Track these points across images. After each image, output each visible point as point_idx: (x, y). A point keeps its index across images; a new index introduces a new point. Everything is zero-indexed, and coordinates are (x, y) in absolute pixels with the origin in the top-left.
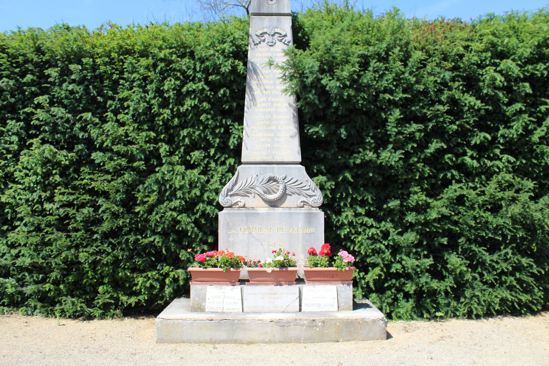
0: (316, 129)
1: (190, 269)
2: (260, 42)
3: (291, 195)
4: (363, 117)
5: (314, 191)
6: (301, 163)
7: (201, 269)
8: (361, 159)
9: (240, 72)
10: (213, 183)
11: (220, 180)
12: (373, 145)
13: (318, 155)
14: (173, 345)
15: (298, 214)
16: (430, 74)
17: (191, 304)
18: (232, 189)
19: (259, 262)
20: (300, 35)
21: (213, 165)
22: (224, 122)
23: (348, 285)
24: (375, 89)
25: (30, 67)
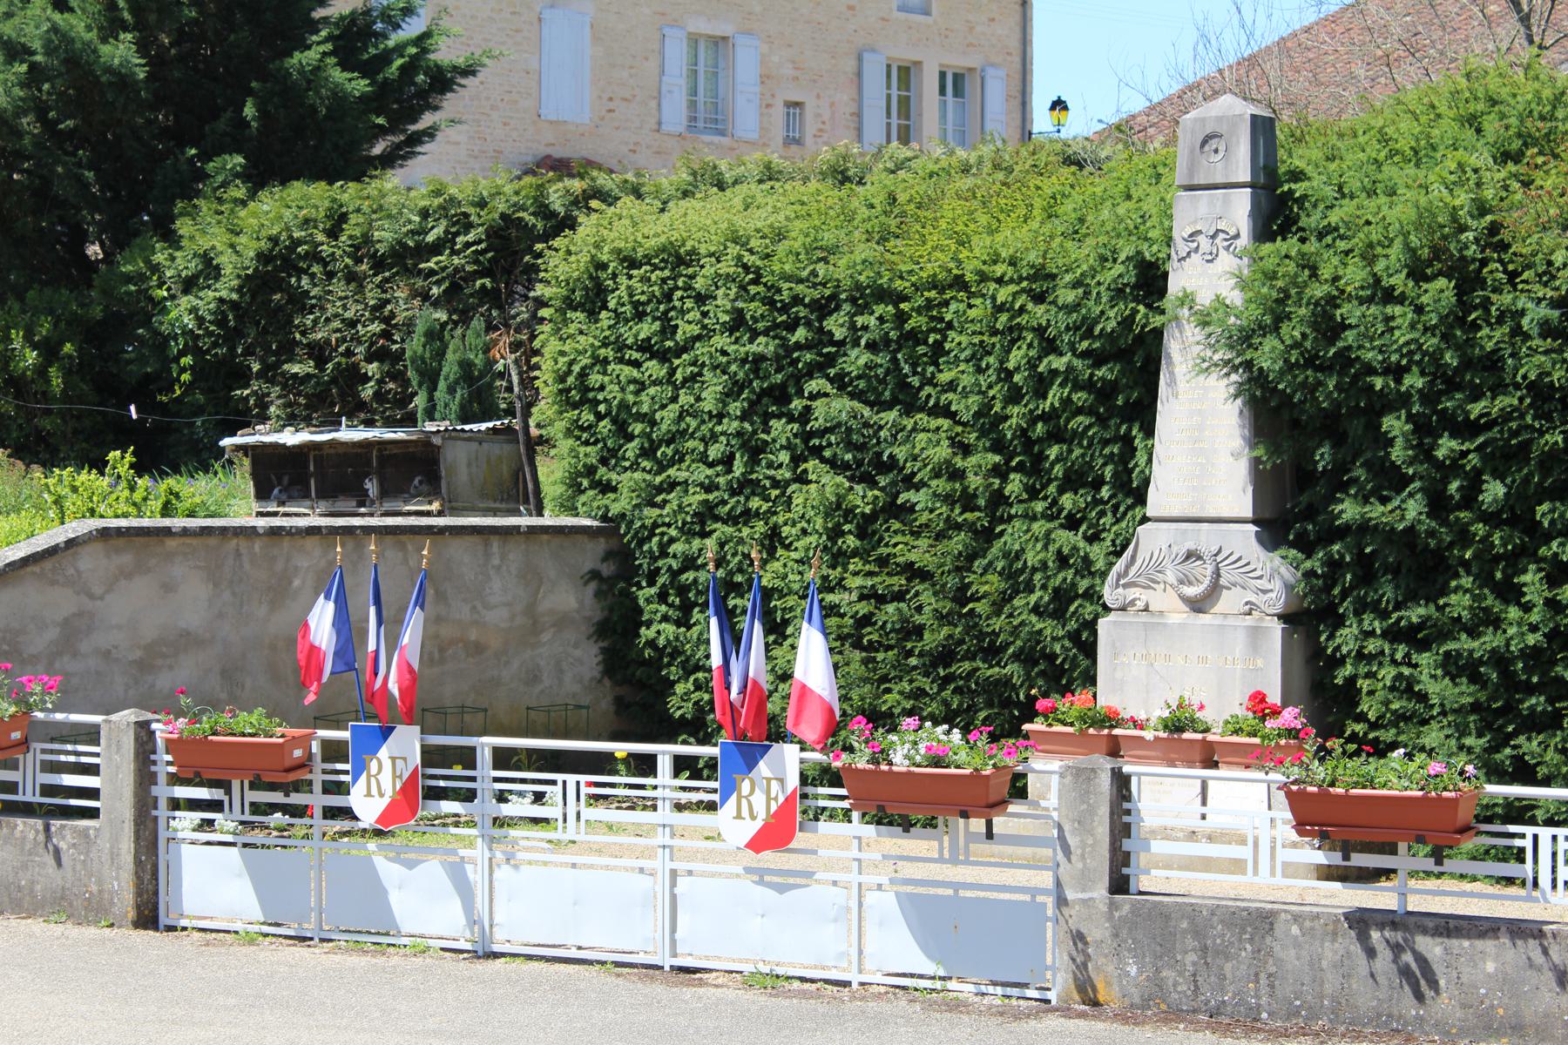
3: (1230, 589)
6: (1255, 522)
25: (803, 312)
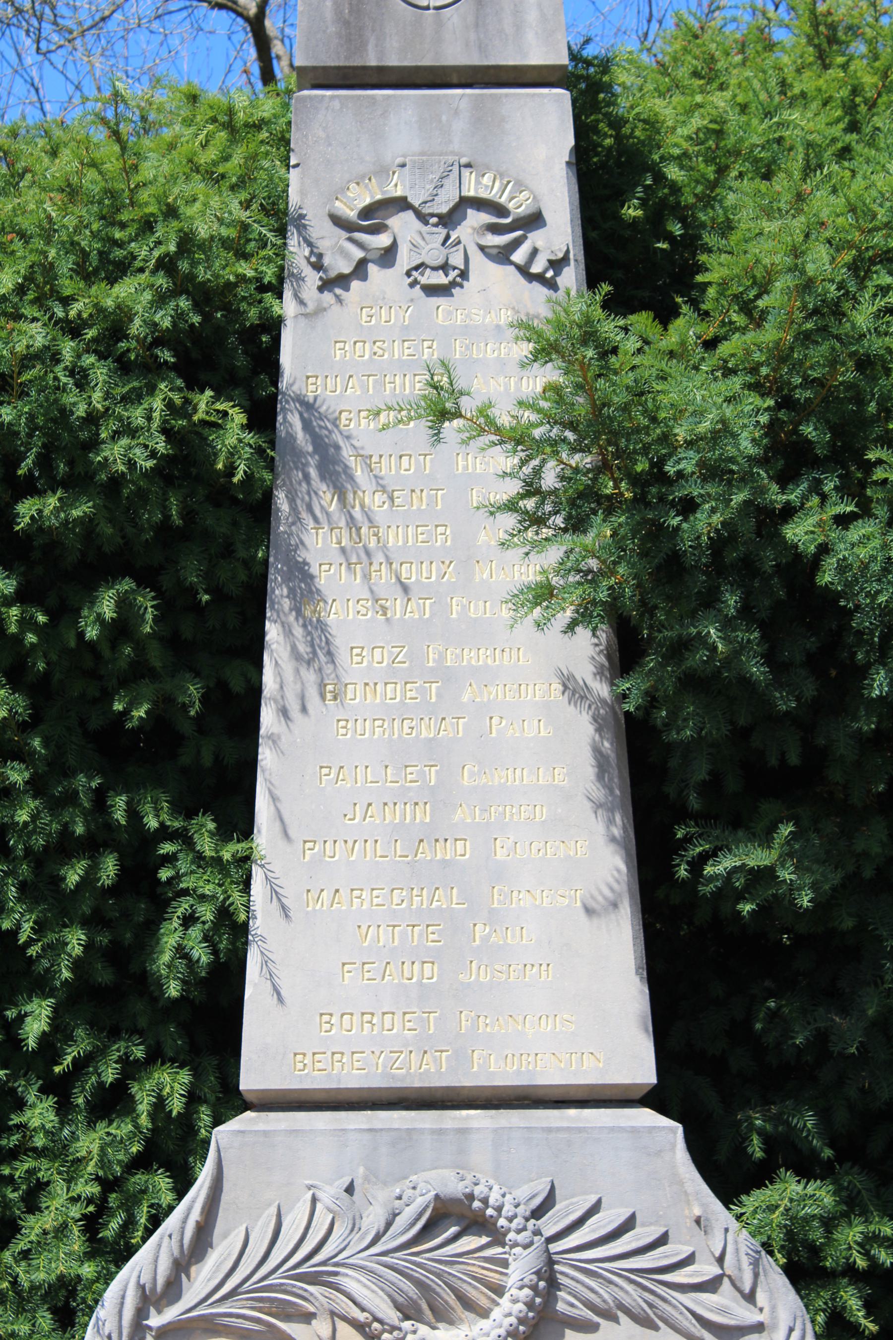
2: (360, 270)
3: (590, 1327)
5: (750, 1298)
9: (231, 470)
10: (40, 1245)
20: (632, 211)
22: (120, 815)
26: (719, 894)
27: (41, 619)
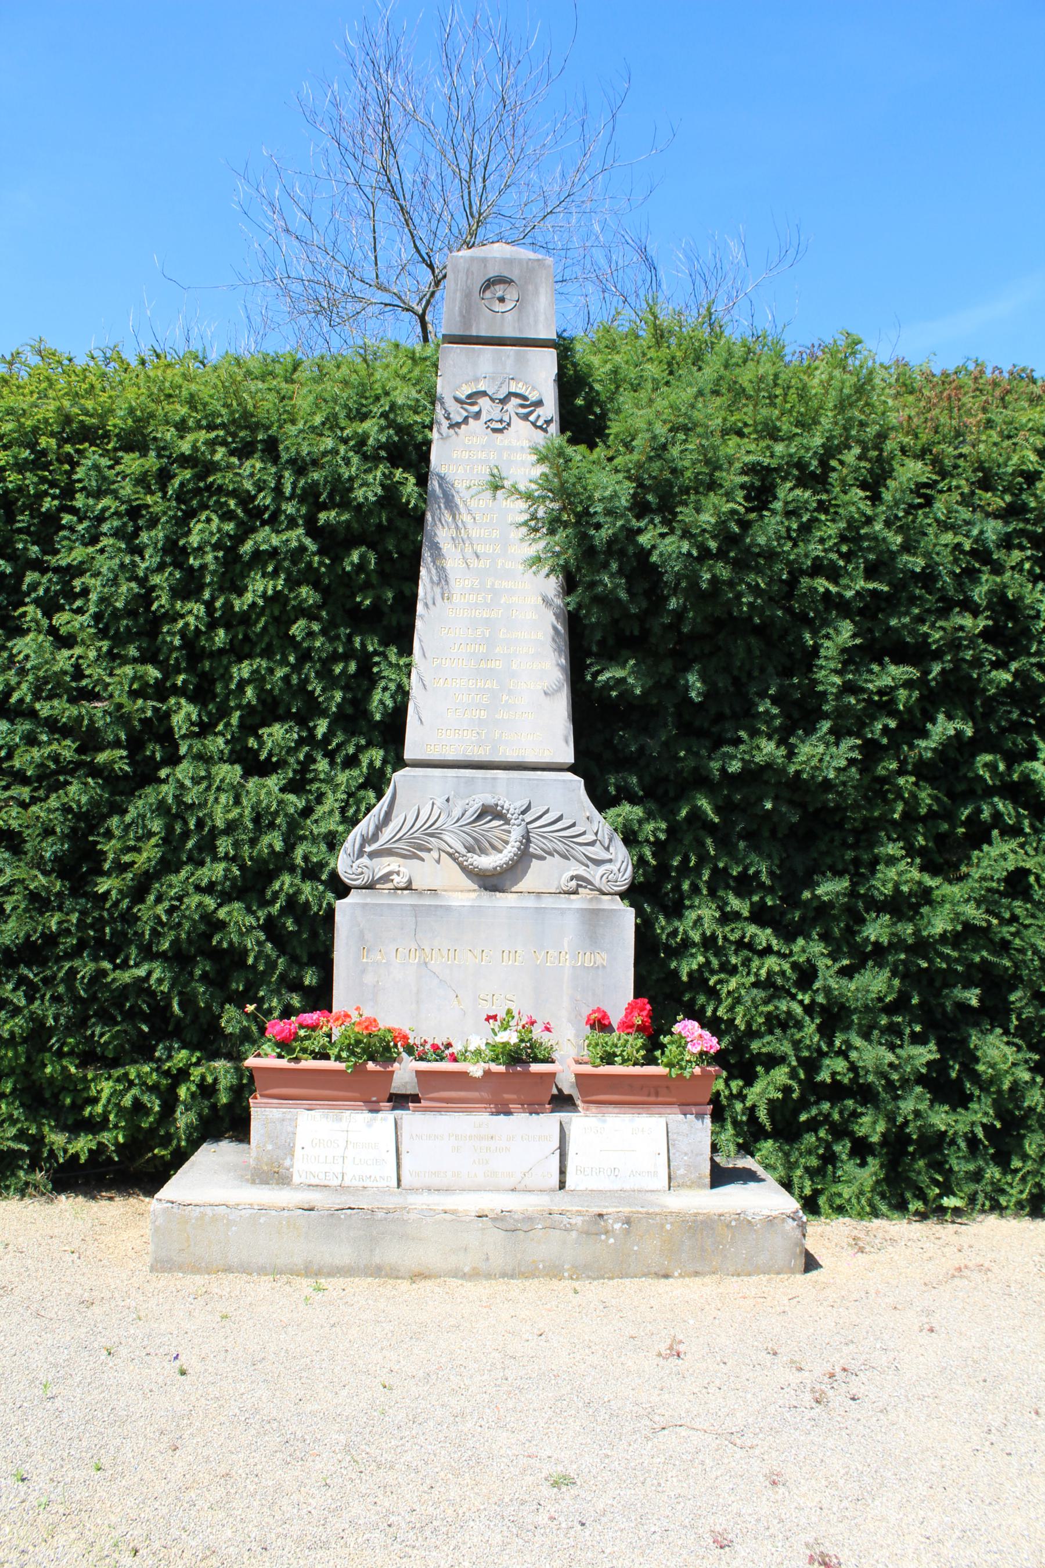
0: (620, 673)
1: (251, 1062)
2: (466, 420)
3: (542, 858)
4: (753, 640)
5: (607, 849)
6: (573, 769)
7: (283, 1063)
8: (742, 759)
9: (408, 502)
11: (343, 810)
12: (777, 722)
13: (620, 747)
14: (199, 1279)
15: (562, 911)
16: (945, 526)
17: (252, 1163)
18: (375, 837)
19: (449, 1045)
20: (580, 402)
21: (322, 765)
22: (357, 645)
23: (700, 1116)
24: (789, 563)
26: (603, 687)
27: (327, 561)
